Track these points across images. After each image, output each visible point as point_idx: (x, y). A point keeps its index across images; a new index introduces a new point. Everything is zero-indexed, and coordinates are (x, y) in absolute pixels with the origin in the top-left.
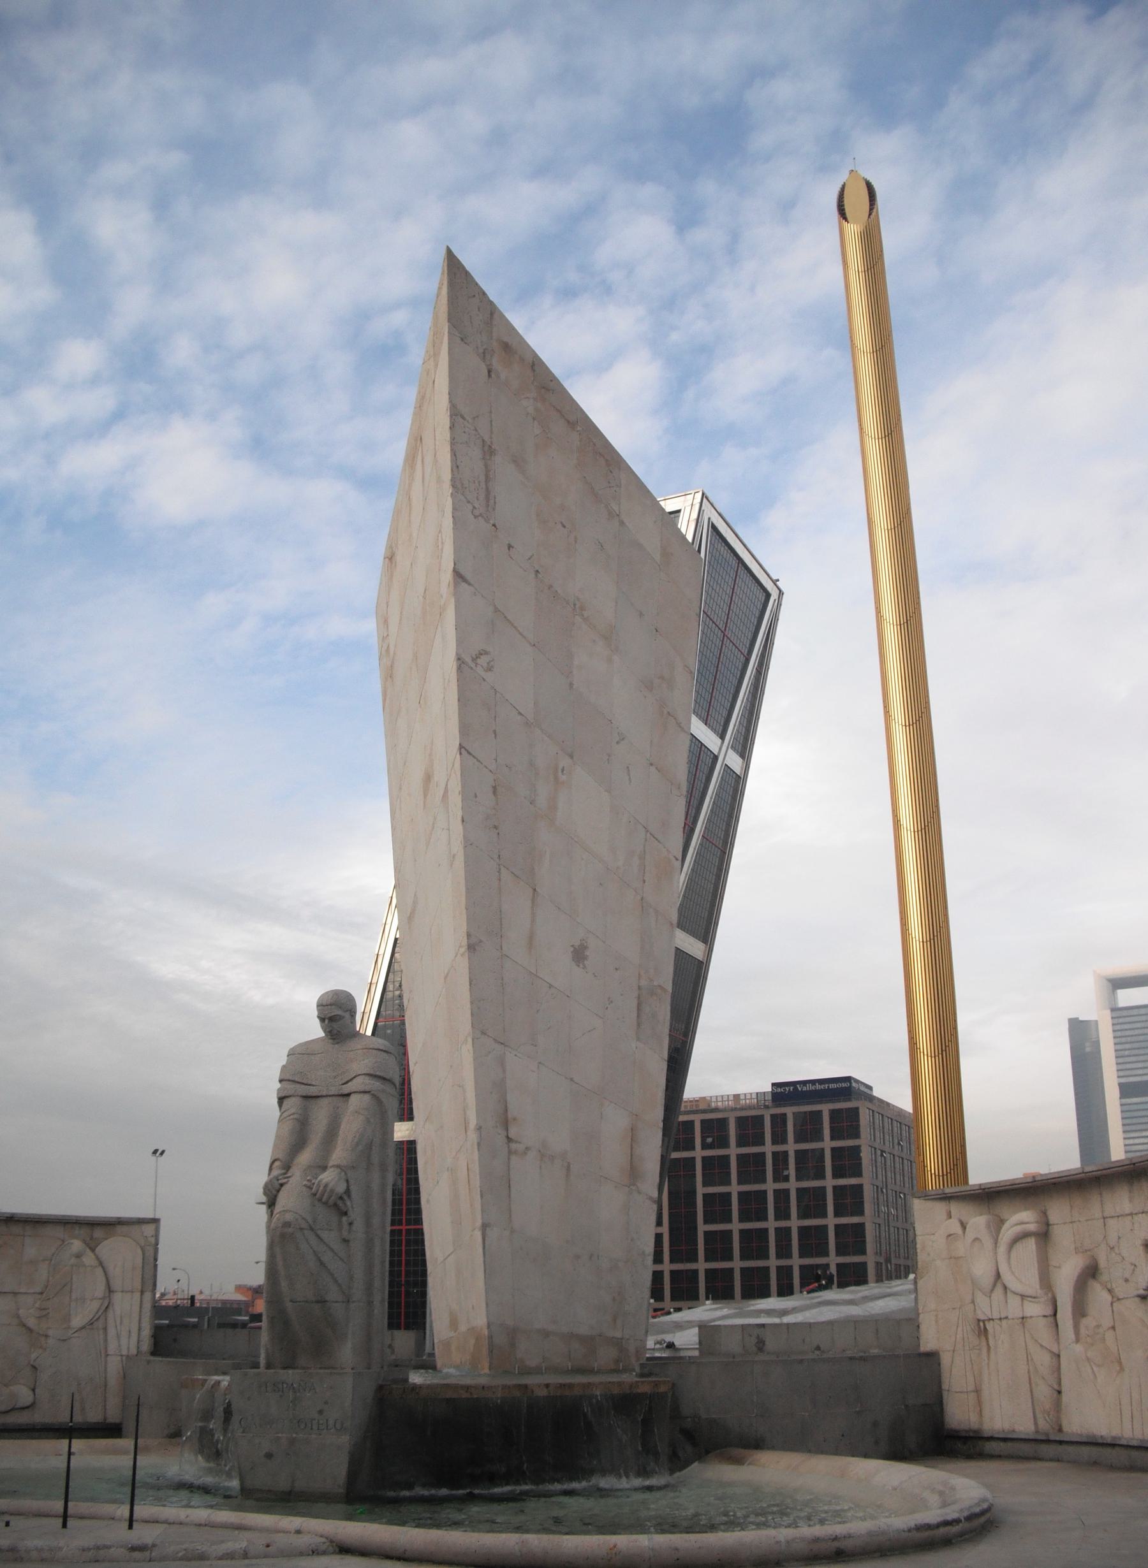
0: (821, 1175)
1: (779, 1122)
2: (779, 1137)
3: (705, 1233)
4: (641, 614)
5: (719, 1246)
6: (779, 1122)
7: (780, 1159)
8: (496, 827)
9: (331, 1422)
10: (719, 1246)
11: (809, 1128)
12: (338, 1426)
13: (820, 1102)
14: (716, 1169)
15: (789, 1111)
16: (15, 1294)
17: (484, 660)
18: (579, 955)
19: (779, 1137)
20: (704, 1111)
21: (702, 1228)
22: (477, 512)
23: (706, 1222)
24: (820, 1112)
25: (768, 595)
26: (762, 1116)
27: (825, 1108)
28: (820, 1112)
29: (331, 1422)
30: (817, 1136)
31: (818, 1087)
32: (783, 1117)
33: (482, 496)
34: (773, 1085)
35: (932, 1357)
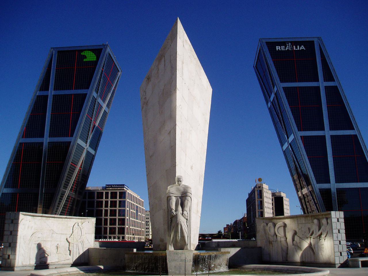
0: (116, 207)
1: (107, 194)
4: (203, 100)
6: (107, 194)
7: (107, 202)
8: (181, 141)
9: (188, 260)
11: (114, 195)
12: (190, 261)
16: (66, 234)
17: (180, 107)
18: (192, 168)
19: (107, 197)
22: (181, 76)
24: (117, 192)
25: (119, 71)
26: (103, 193)
28: (117, 192)
29: (188, 260)
33: (181, 72)
34: (106, 185)
35: (260, 248)
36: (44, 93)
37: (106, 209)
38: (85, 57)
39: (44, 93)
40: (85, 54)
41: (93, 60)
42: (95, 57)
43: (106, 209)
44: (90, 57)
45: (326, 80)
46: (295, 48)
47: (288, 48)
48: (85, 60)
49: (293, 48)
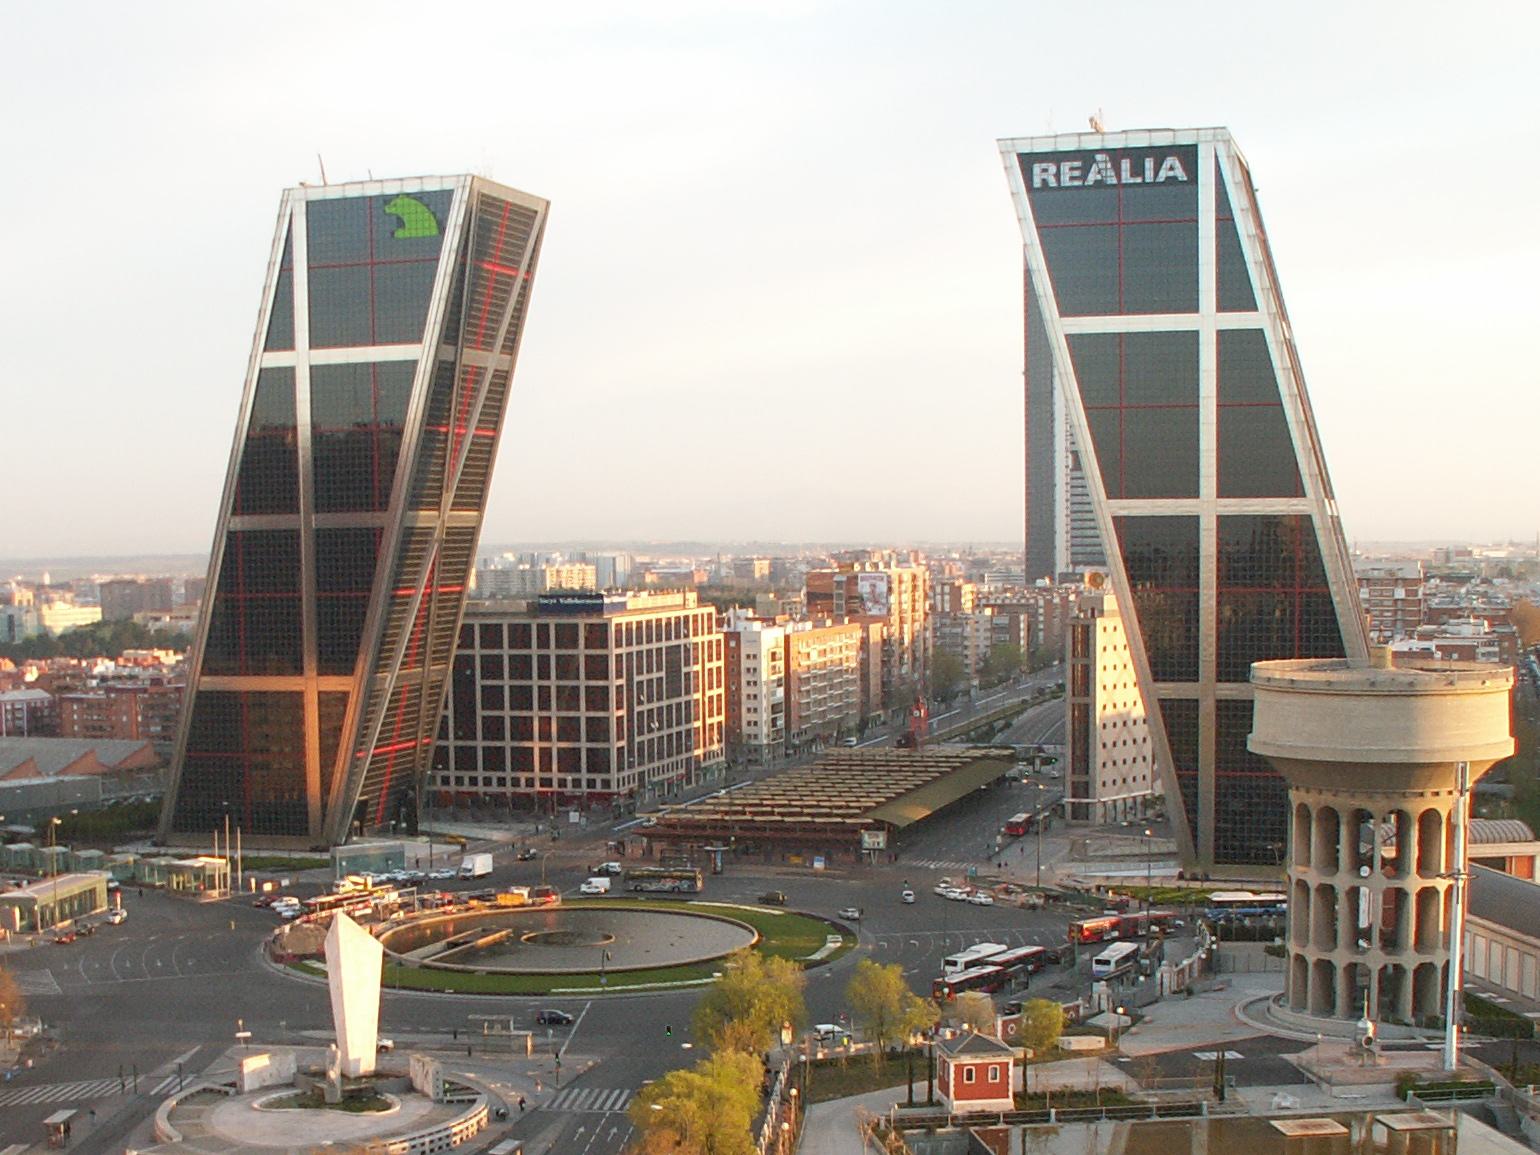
1: (543, 629)
2: (544, 642)
3: (484, 717)
5: (494, 728)
6: (543, 629)
10: (494, 728)
11: (567, 636)
13: (575, 616)
14: (492, 667)
15: (552, 622)
19: (544, 642)
20: (484, 615)
21: (480, 713)
23: (483, 708)
27: (582, 622)
30: (575, 644)
31: (577, 601)
32: (547, 625)
36: (278, 359)
37: (545, 683)
38: (400, 223)
39: (278, 359)
40: (399, 211)
41: (427, 233)
42: (434, 224)
43: (545, 683)
44: (419, 224)
45: (1222, 306)
46: (1126, 177)
47: (1099, 172)
48: (400, 234)
49: (1118, 175)
